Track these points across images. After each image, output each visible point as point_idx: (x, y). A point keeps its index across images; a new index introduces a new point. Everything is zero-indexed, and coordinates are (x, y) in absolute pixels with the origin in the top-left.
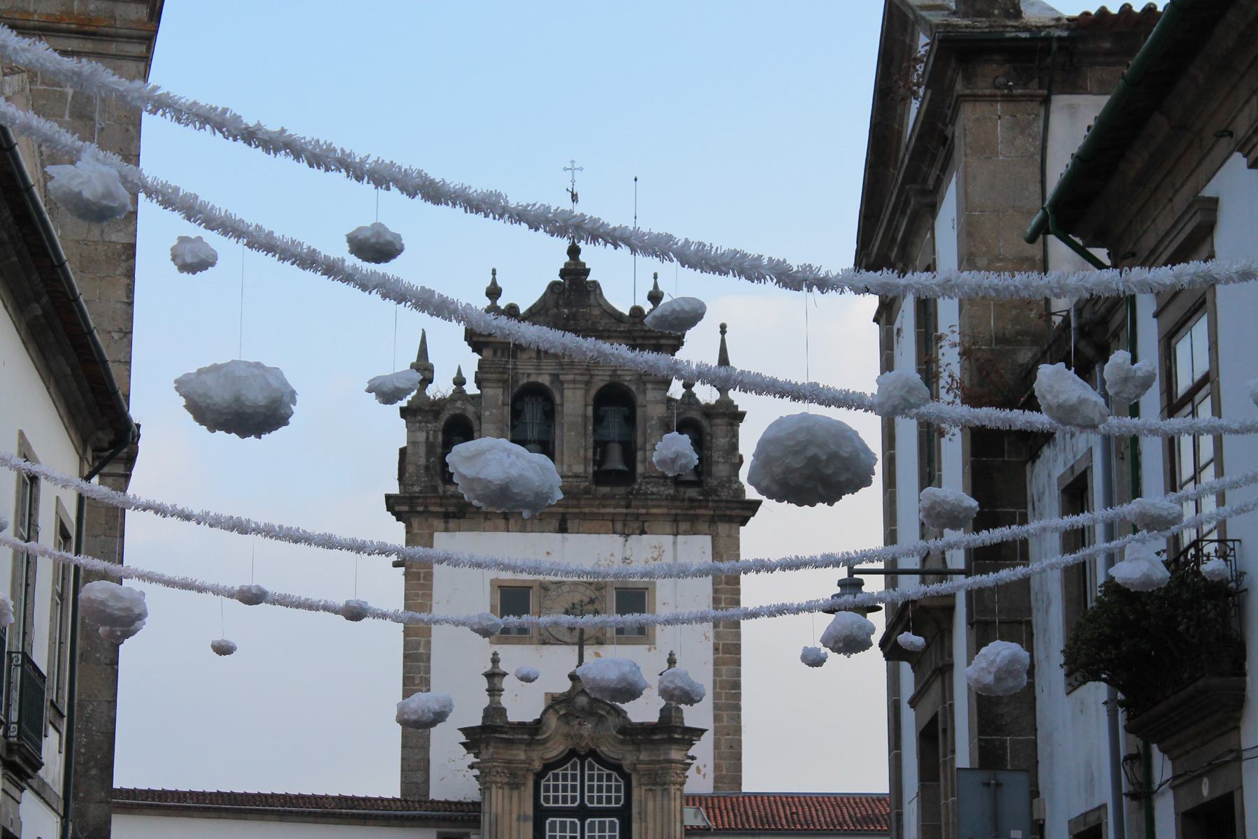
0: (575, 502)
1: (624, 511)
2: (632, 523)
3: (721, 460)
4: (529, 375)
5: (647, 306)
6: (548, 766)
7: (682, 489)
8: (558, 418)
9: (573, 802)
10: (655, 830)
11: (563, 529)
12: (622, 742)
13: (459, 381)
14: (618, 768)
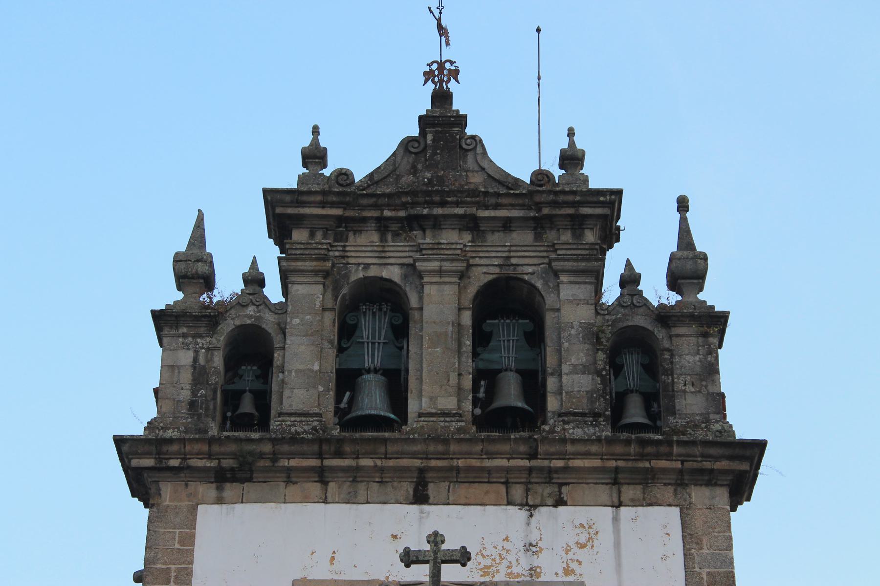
0: (440, 448)
1: (526, 463)
2: (542, 485)
3: (690, 388)
4: (367, 266)
5: (557, 173)
8: (413, 331)
11: (420, 498)
13: (254, 280)
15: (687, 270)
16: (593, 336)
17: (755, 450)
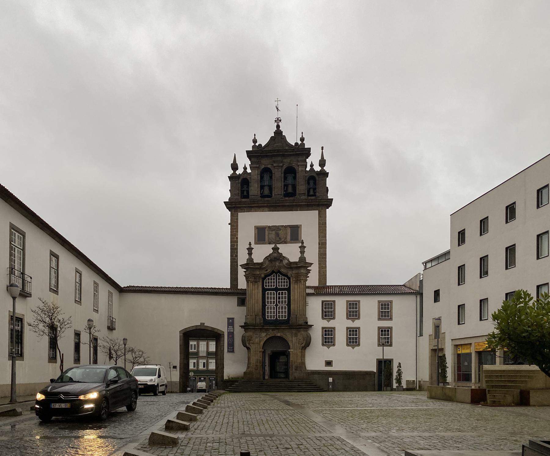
5: (300, 142)
6: (266, 276)
7: (310, 198)
9: (274, 286)
12: (287, 268)
13: (245, 168)
14: (287, 276)
15: (322, 163)
17: (332, 200)
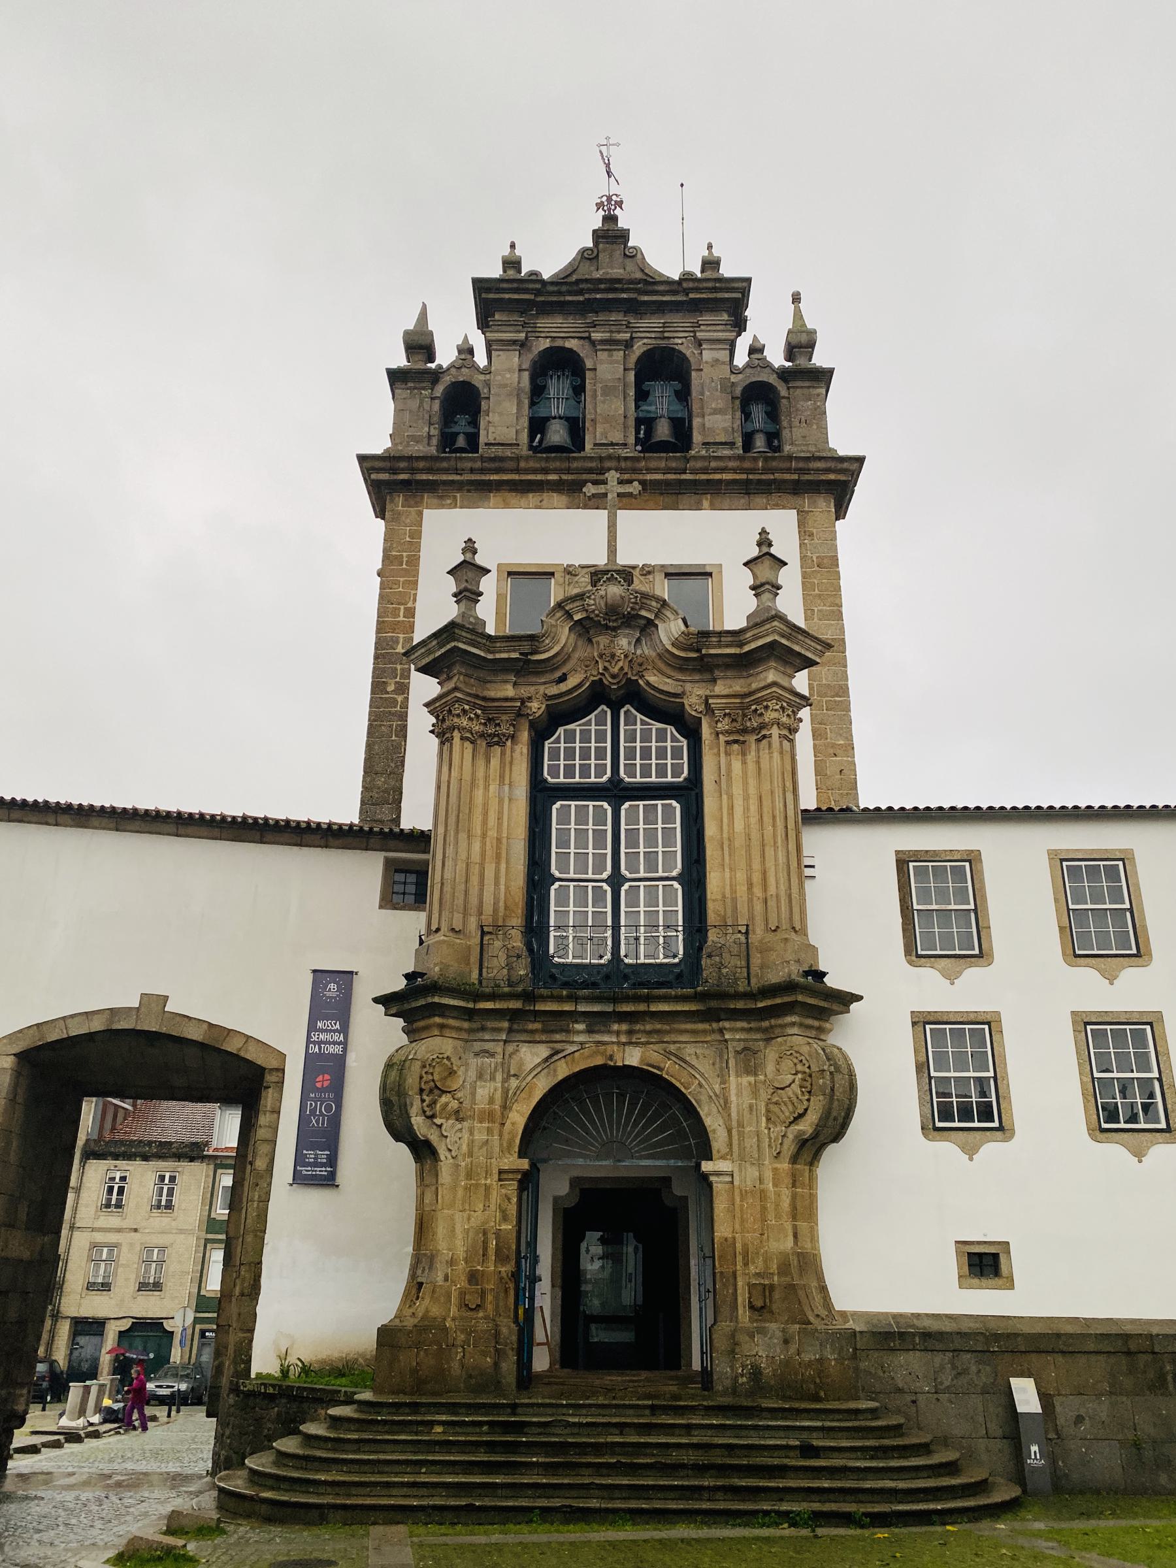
10: (746, 809)
13: (467, 351)
15: (800, 344)
16: (727, 387)
